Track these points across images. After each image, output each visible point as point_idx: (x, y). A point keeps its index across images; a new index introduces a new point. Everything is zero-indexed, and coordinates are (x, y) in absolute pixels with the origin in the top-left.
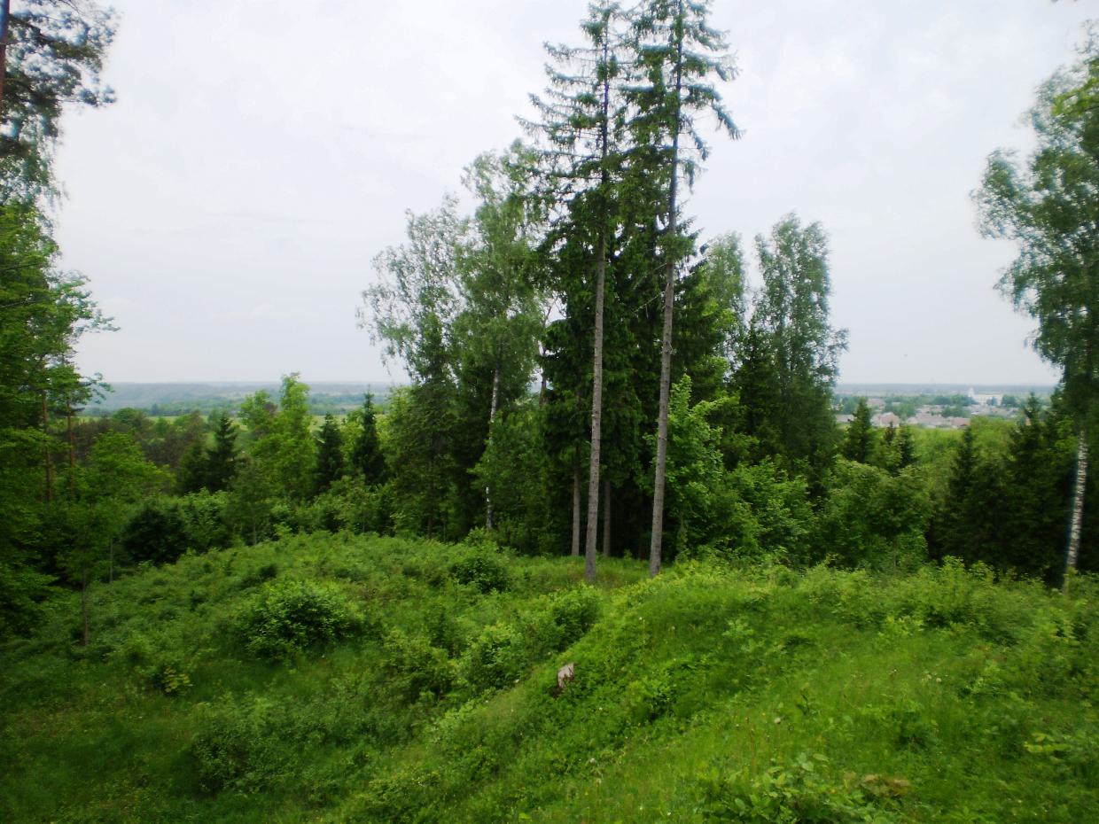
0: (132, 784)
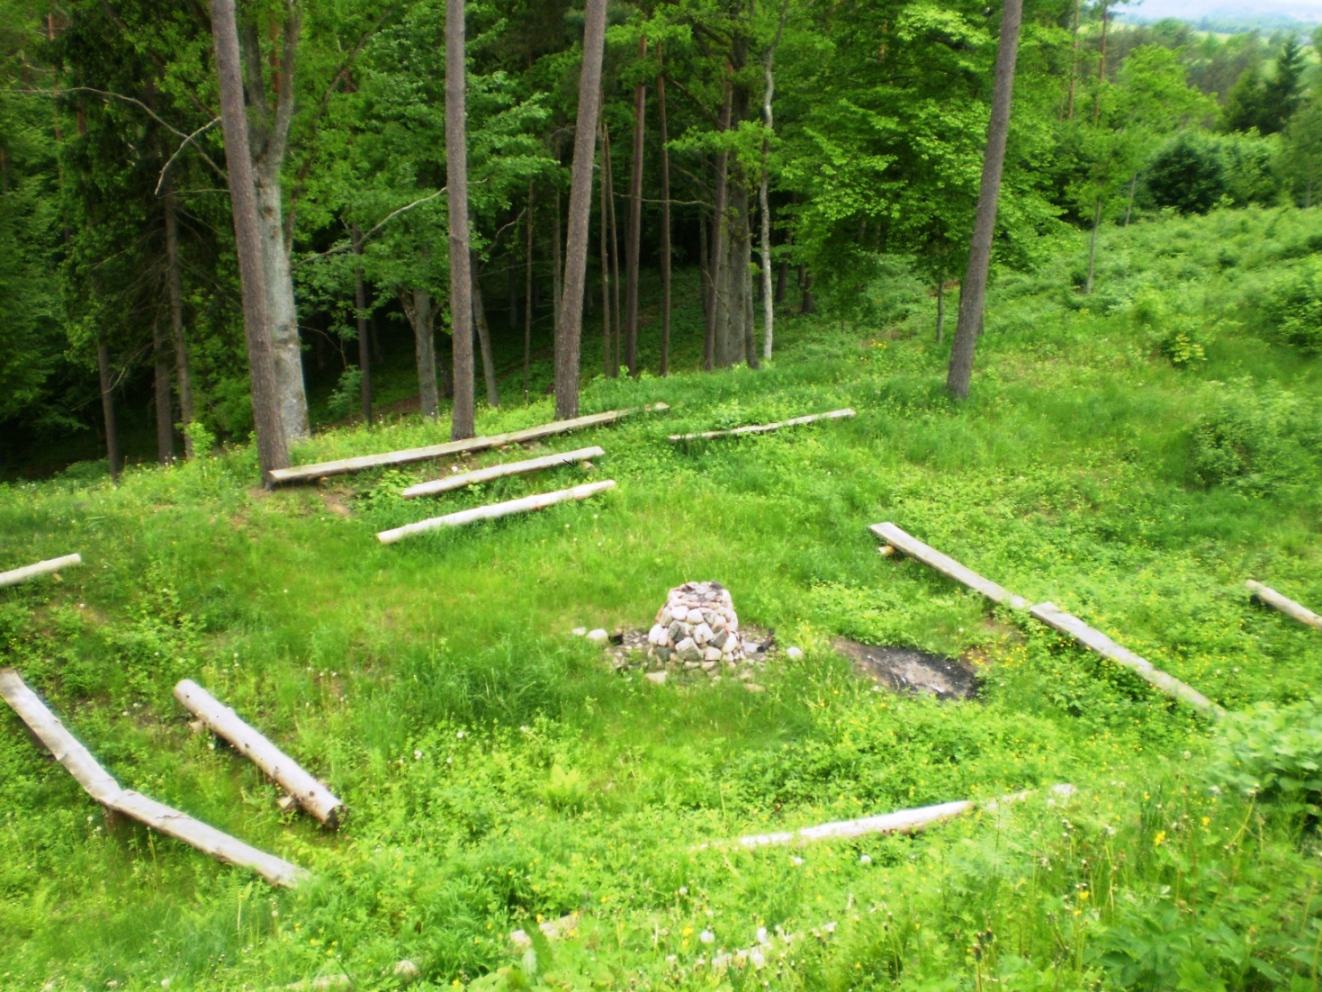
0: (1117, 456)
